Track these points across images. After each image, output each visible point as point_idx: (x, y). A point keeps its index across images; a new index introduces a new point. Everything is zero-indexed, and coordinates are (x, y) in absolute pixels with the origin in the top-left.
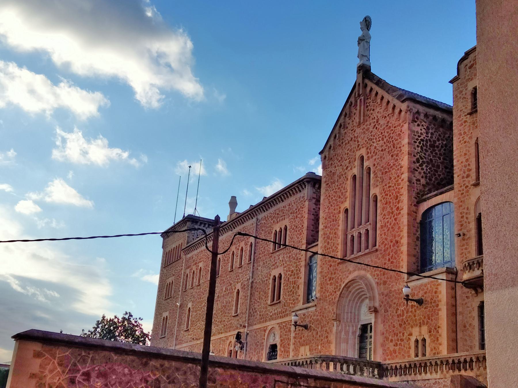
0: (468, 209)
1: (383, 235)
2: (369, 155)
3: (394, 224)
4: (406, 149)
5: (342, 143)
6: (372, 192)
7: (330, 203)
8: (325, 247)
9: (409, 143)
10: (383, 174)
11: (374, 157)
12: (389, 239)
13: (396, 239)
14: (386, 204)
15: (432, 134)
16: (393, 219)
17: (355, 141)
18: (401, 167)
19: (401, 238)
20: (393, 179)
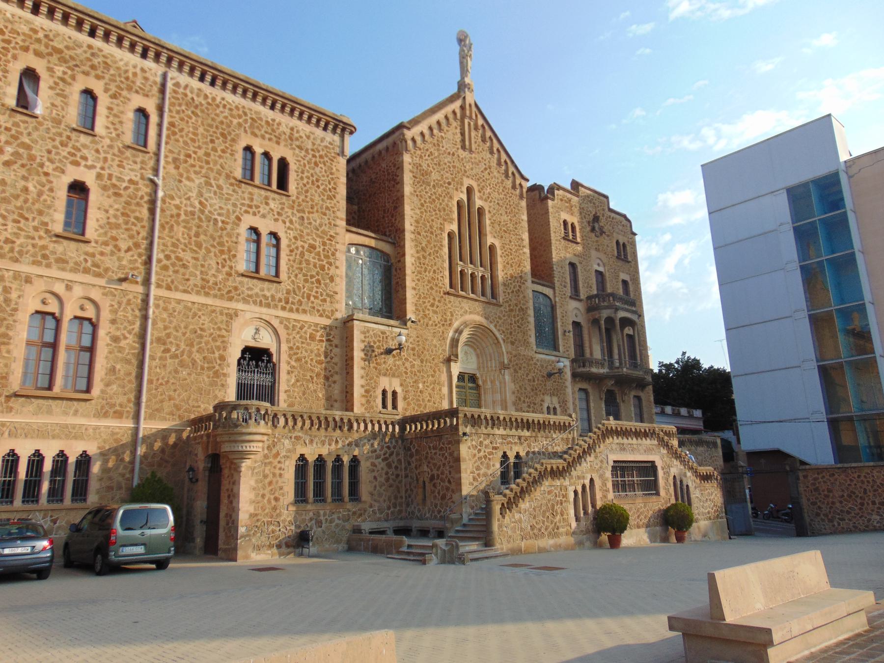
6: (490, 240)
8: (419, 258)
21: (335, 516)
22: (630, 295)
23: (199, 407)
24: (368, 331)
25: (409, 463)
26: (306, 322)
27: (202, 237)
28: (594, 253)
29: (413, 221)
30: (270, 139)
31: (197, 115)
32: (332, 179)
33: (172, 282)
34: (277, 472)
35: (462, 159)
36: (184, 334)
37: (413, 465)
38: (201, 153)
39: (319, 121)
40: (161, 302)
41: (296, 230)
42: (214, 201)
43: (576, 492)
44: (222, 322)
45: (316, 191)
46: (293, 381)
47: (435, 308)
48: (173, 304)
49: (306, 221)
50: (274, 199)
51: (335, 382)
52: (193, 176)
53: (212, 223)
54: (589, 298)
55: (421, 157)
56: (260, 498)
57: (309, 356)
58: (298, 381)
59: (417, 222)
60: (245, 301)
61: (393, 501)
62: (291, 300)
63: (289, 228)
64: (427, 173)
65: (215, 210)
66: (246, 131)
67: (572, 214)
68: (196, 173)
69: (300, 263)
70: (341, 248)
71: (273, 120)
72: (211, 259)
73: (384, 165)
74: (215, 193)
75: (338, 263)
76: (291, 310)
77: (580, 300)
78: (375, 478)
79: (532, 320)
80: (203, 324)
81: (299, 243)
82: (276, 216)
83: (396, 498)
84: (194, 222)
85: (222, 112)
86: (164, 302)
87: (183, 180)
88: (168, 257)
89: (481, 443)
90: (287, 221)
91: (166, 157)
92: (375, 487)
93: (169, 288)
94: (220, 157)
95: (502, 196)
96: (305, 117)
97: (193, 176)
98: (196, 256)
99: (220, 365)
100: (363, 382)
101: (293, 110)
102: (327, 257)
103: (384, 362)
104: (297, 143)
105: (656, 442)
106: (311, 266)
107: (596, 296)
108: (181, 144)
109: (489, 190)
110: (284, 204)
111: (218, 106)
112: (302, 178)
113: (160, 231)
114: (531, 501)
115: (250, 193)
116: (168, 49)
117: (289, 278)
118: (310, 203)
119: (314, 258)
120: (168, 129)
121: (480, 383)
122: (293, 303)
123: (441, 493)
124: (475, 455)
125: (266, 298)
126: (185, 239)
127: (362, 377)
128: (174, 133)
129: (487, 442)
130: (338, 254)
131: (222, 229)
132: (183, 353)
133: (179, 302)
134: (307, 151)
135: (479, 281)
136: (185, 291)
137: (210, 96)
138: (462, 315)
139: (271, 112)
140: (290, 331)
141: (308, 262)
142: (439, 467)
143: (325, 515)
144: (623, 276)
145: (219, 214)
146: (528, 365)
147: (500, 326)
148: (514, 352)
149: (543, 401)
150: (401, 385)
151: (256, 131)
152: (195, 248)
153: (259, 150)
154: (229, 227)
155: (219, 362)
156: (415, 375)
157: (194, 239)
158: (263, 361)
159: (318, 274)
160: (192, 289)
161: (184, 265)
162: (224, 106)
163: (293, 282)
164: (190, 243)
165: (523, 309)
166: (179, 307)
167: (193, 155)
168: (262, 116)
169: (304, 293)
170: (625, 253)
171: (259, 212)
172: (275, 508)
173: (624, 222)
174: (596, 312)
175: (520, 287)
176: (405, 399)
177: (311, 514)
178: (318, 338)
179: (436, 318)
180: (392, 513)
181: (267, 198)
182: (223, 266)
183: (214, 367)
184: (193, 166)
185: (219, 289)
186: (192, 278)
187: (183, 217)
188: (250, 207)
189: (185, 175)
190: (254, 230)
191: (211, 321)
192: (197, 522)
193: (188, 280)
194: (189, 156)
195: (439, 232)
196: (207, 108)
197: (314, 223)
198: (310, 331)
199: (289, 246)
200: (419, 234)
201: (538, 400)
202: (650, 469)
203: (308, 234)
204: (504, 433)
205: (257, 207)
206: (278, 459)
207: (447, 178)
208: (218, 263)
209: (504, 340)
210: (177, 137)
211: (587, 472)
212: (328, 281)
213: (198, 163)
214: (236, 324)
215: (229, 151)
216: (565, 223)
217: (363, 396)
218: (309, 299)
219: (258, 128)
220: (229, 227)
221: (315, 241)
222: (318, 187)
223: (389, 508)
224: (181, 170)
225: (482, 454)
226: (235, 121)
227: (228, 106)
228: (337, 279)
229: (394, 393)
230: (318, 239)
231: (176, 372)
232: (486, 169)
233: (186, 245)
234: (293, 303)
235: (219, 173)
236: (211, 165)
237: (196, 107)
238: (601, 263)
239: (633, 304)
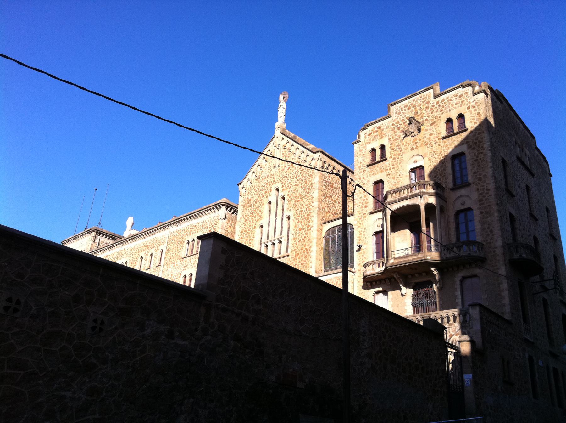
0: (365, 229)
1: (295, 245)
3: (305, 237)
4: (317, 186)
5: (259, 178)
7: (246, 220)
9: (319, 182)
11: (288, 190)
12: (300, 247)
13: (307, 247)
14: (298, 222)
15: (332, 178)
16: (304, 233)
17: (271, 177)
18: (312, 198)
19: (311, 247)
20: (304, 205)
59: (242, 232)
109: (289, 181)
175: (306, 234)
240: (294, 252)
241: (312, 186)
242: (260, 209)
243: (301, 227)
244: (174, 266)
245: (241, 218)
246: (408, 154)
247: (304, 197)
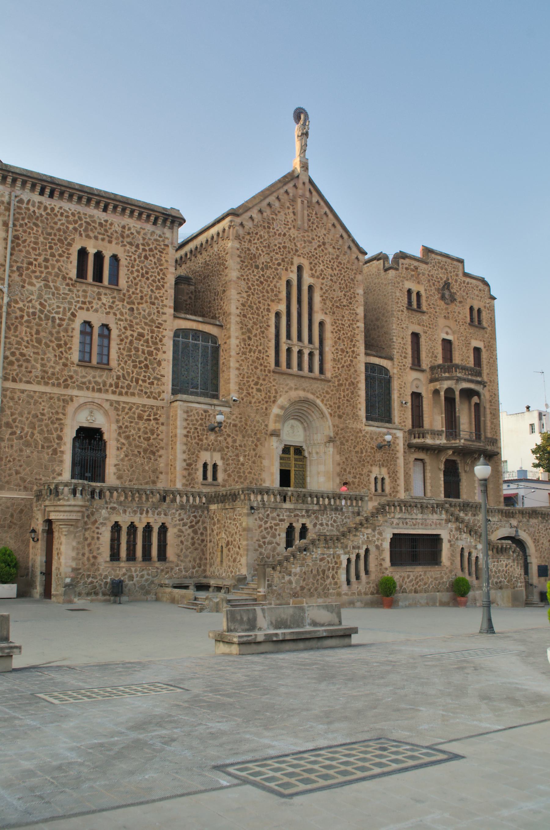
2: (313, 272)
8: (244, 340)
10: (333, 305)
12: (344, 376)
19: (358, 382)
21: (145, 572)
22: (482, 363)
23: (41, 479)
24: (192, 411)
25: (213, 531)
26: (134, 404)
27: (42, 334)
28: (441, 322)
29: (239, 304)
30: (103, 240)
31: (36, 225)
32: (161, 270)
33: (17, 375)
34: (96, 536)
35: (294, 239)
36: (27, 419)
37: (215, 532)
38: (41, 259)
39: (149, 216)
40: (8, 393)
41: (126, 320)
42: (53, 301)
43: (349, 560)
44: (59, 407)
45: (145, 284)
46: (122, 456)
47: (258, 387)
48: (18, 394)
49: (135, 312)
50: (105, 294)
51: (160, 456)
52: (34, 281)
53: (50, 321)
54: (432, 368)
55: (250, 241)
56: (80, 556)
57: (136, 434)
58: (126, 456)
59: (243, 305)
60: (80, 388)
61: (198, 561)
62: (120, 384)
63: (120, 320)
64: (254, 257)
65: (53, 309)
66: (81, 235)
67: (419, 283)
68: (37, 278)
69: (130, 350)
70: (168, 335)
71: (106, 221)
72: (49, 352)
73: (216, 249)
74: (53, 294)
75: (164, 349)
76: (121, 394)
77: (423, 371)
78: (182, 542)
79: (362, 393)
80: (43, 410)
81: (129, 333)
82: (108, 310)
83: (201, 559)
84: (35, 322)
85: (60, 220)
86: (11, 392)
87: (26, 285)
88: (13, 354)
89: (268, 515)
90: (117, 313)
91: (11, 266)
92: (182, 550)
93: (14, 380)
94: (58, 261)
95: (336, 272)
96: (136, 214)
97: (34, 281)
98: (36, 351)
99: (58, 444)
100: (185, 456)
101: (124, 210)
102: (156, 343)
103: (206, 438)
104: (129, 240)
105: (444, 516)
106: (140, 353)
107: (439, 366)
108: (24, 254)
109: (321, 267)
110: (115, 298)
111: (56, 215)
112: (132, 272)
113: (6, 332)
114: (302, 565)
115: (84, 291)
116: (13, 173)
117: (119, 364)
118: (140, 295)
119: (142, 345)
120: (12, 242)
121: (306, 454)
122: (122, 387)
123: (234, 556)
124: (260, 526)
125: (96, 383)
126: (27, 337)
127: (184, 452)
128: (18, 245)
129: (275, 514)
130: (165, 340)
131: (60, 325)
132: (27, 434)
133: (23, 391)
134: (137, 246)
135: (306, 358)
136: (28, 382)
137: (49, 207)
138: (287, 392)
139: (104, 214)
140: (120, 413)
141: (137, 349)
142: (233, 535)
143: (136, 571)
144: (476, 343)
145: (57, 313)
146: (356, 438)
147: (328, 400)
148: (341, 426)
149: (371, 472)
150: (223, 458)
151: (92, 234)
152: (36, 344)
153: (92, 251)
154: (65, 323)
155: (57, 441)
156: (237, 449)
157: (35, 336)
158: (95, 439)
159: (146, 359)
160: (34, 380)
161: (27, 359)
162: (62, 214)
163: (123, 368)
164: (32, 340)
165: (353, 384)
166: (24, 396)
167: (34, 262)
168: (95, 219)
169: (133, 377)
170: (480, 320)
171: (92, 307)
172: (93, 564)
173: (481, 286)
174: (437, 383)
175: (351, 361)
176: (225, 471)
177: (124, 570)
178: (145, 417)
179: (260, 396)
180: (197, 571)
181: (99, 294)
182: (61, 358)
183: (53, 446)
184: (34, 272)
185: (58, 379)
186: (33, 370)
187: (26, 318)
188: (84, 303)
189: (27, 280)
190: (87, 323)
191: (51, 407)
192: (38, 573)
193: (30, 372)
194: (31, 263)
195: (266, 313)
196: (47, 219)
197: (143, 313)
198: (138, 411)
199: (119, 336)
200: (245, 316)
201: (365, 471)
202: (436, 540)
203: (137, 324)
204: (292, 506)
205: (90, 303)
206: (97, 525)
207: (276, 259)
208: (56, 356)
209: (331, 414)
210: (21, 247)
211: (363, 543)
212: (156, 365)
213: (38, 269)
214: (70, 409)
215: (66, 255)
216: (409, 292)
217: (185, 469)
218: (137, 381)
219: (92, 230)
220: (65, 323)
221: (144, 329)
222: (148, 279)
223: (194, 568)
224: (24, 277)
225: (268, 525)
226: (71, 227)
227: (65, 214)
228: (163, 363)
229: (215, 466)
230: (147, 328)
231: (21, 450)
232: (319, 246)
233: (28, 342)
234: (122, 387)
235: (57, 275)
236: (50, 270)
237: (37, 219)
238: (449, 331)
239: (480, 374)
240: (336, 379)
241: (355, 297)
242: (274, 283)
243: (342, 347)
244: (47, 286)
245: (238, 278)
246: (441, 322)
247: (344, 306)
